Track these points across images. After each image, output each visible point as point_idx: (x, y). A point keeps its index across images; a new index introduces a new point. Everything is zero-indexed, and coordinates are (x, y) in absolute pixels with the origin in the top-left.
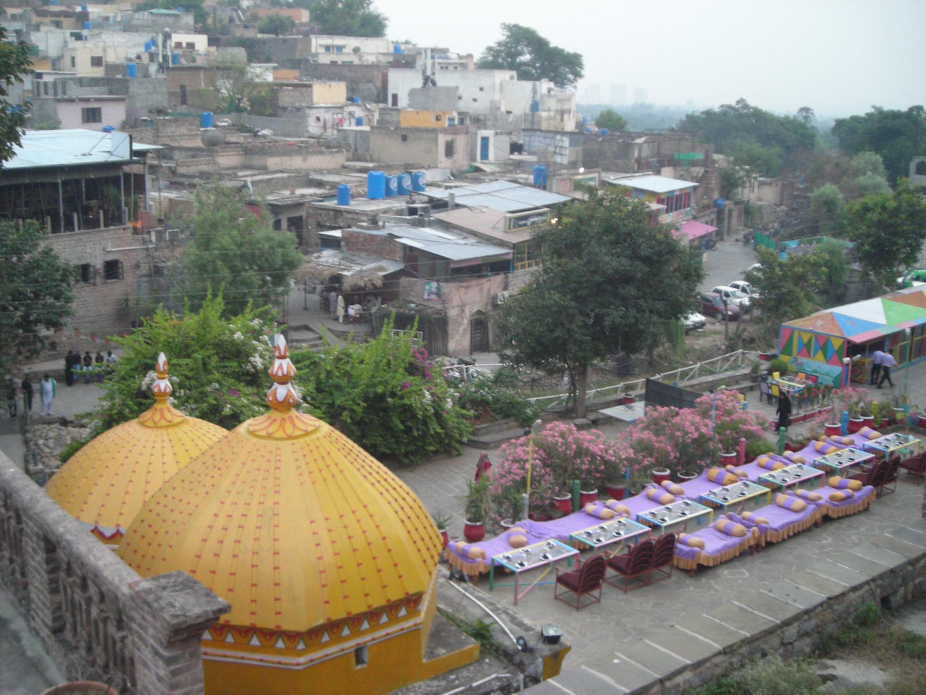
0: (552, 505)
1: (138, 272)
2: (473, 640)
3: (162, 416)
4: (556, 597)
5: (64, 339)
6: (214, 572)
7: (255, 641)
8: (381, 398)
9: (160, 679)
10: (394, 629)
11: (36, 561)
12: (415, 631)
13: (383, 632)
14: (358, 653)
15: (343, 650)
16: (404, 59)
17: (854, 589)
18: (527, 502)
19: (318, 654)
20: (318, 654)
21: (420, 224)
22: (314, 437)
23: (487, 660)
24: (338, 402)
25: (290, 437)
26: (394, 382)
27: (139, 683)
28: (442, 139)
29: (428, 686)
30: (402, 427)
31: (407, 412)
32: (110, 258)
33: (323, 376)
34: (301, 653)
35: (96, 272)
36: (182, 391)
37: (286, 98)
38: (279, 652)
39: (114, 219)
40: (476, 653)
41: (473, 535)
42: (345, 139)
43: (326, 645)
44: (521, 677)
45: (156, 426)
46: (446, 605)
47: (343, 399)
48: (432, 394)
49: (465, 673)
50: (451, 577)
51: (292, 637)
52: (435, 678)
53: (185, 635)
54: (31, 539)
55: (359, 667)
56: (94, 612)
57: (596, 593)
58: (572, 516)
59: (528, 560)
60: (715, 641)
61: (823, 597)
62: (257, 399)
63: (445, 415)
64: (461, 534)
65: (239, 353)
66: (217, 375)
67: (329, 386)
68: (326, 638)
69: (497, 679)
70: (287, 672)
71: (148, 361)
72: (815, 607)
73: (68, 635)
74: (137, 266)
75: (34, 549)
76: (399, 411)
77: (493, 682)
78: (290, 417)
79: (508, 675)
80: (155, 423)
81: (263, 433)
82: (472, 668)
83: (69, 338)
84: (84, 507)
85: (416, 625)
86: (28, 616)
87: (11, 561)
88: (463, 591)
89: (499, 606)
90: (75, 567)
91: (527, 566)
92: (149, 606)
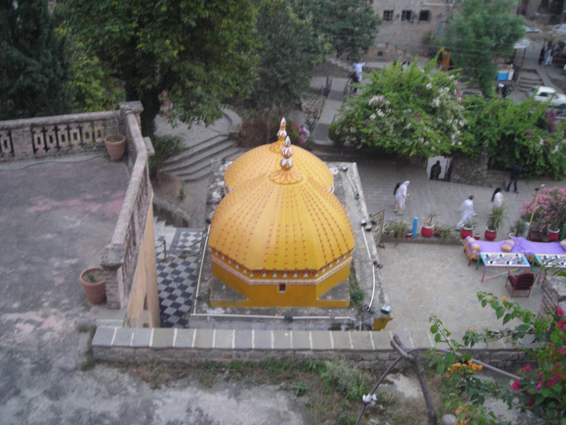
0: (545, 232)
2: (349, 298)
3: (278, 147)
4: (506, 286)
5: (388, 51)
8: (512, 136)
10: (300, 281)
12: (313, 286)
13: (295, 281)
18: (528, 228)
19: (260, 281)
20: (260, 281)
22: (292, 186)
23: (353, 309)
24: (485, 134)
25: (281, 183)
26: (521, 130)
30: (518, 156)
31: (525, 149)
32: (425, 9)
33: (482, 116)
34: (251, 278)
35: (415, 17)
36: (390, 110)
38: (244, 274)
40: (348, 304)
41: (490, 237)
43: (264, 278)
44: (361, 323)
45: (274, 151)
47: (488, 132)
48: (545, 142)
49: (338, 311)
50: (375, 263)
51: (248, 271)
55: (282, 292)
57: (528, 292)
58: (552, 244)
59: (498, 260)
60: (335, 344)
62: (430, 123)
63: (549, 156)
64: (482, 235)
65: (429, 95)
66: (412, 105)
67: (486, 122)
68: (264, 275)
69: (349, 320)
74: (440, 16)
76: (521, 147)
79: (355, 320)
81: (272, 178)
82: (343, 310)
83: (391, 51)
88: (374, 272)
89: (382, 286)
91: (494, 264)
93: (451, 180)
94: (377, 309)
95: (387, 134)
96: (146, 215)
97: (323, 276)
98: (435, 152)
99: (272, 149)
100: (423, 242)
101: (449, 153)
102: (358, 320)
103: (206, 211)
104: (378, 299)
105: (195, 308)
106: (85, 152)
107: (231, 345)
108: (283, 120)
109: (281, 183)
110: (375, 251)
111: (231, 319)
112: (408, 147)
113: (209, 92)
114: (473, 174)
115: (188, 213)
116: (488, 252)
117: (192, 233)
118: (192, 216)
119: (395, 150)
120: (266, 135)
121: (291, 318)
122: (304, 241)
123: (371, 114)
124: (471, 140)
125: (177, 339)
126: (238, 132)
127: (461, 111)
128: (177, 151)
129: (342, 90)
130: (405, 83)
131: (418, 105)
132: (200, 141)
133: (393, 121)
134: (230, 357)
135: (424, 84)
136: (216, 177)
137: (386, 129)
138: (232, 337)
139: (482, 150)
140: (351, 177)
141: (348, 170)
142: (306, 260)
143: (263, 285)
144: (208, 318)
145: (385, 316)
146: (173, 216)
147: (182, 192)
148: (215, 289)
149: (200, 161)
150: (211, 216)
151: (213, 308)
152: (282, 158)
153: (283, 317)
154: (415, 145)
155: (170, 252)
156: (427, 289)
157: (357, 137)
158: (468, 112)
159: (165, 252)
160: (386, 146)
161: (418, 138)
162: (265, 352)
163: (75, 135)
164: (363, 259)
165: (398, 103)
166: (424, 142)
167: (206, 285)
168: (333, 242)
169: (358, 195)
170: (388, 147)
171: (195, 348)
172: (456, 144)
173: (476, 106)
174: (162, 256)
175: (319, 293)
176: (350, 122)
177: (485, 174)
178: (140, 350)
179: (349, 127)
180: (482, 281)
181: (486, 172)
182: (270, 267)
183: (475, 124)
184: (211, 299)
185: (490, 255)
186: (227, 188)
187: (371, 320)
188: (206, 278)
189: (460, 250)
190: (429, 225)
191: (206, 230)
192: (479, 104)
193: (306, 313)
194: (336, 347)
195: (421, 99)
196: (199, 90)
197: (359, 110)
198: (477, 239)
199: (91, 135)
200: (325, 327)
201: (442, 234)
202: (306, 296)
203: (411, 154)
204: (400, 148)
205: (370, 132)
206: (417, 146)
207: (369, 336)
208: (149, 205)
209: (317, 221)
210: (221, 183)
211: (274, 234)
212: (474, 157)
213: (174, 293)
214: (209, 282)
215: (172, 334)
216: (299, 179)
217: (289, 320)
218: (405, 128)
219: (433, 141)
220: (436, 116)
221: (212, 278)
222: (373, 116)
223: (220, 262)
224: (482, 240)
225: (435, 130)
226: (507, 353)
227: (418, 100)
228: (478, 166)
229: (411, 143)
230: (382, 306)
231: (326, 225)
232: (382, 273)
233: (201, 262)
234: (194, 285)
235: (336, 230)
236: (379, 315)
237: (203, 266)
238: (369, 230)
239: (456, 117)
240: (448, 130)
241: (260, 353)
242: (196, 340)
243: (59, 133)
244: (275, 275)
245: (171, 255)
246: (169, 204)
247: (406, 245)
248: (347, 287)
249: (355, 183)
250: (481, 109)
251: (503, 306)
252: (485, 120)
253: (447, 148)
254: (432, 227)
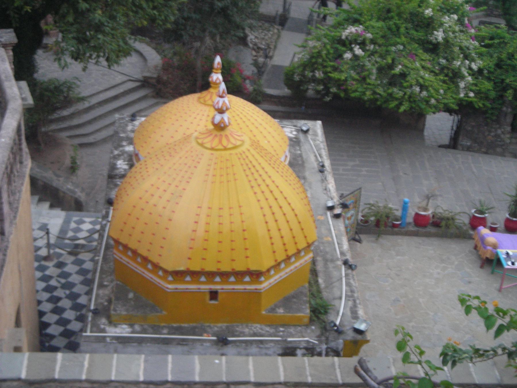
2: (308, 311)
6: (138, 219)
12: (257, 293)
15: (199, 289)
19: (181, 286)
20: (181, 286)
22: (228, 152)
23: (313, 327)
24: (507, 81)
25: (212, 149)
29: (261, 329)
33: (504, 56)
34: (170, 282)
36: (372, 47)
38: (160, 277)
40: (306, 320)
44: (324, 347)
45: (205, 104)
46: (325, 281)
47: (512, 79)
49: (292, 330)
50: (346, 263)
51: (165, 271)
52: (269, 326)
55: (213, 302)
60: (285, 376)
62: (429, 66)
64: (501, 225)
65: (429, 25)
66: (403, 39)
67: (509, 65)
69: (308, 342)
70: (162, 290)
71: (358, 17)
77: (303, 342)
78: (221, 135)
79: (316, 342)
80: (205, 101)
81: (200, 141)
82: (299, 328)
84: (144, 145)
85: (256, 289)
88: (344, 274)
89: (356, 295)
93: (460, 147)
94: (348, 328)
95: (368, 81)
96: (20, 192)
97: (272, 280)
98: (435, 107)
99: (202, 100)
100: (416, 234)
101: (456, 108)
102: (320, 342)
103: (108, 187)
104: (349, 313)
105: (89, 326)
107: (138, 376)
108: (218, 59)
109: (212, 149)
110: (346, 246)
111: (140, 341)
112: (397, 99)
113: (112, 18)
114: (490, 138)
115: (83, 190)
116: (509, 249)
117: (87, 220)
118: (88, 194)
119: (379, 103)
120: (196, 80)
121: (226, 339)
122: (244, 230)
123: (345, 52)
124: (488, 90)
125: (61, 368)
126: (155, 76)
127: (475, 48)
128: (68, 102)
129: (305, 17)
130: (394, 8)
131: (413, 39)
132: (101, 89)
133: (377, 62)
135: (420, 10)
136: (122, 139)
137: (366, 73)
138: (139, 365)
139: (503, 103)
140: (314, 140)
141: (310, 132)
142: (247, 257)
143: (185, 292)
144: (108, 340)
145: (359, 337)
146: (61, 194)
147: (74, 161)
148: (117, 299)
149: (101, 117)
150: (113, 194)
151: (115, 326)
152: (216, 113)
153: (215, 338)
154: (406, 97)
155: (56, 246)
156: (421, 300)
157: (325, 85)
158: (484, 49)
159: (49, 246)
160: (366, 98)
161: (411, 86)
164: (329, 256)
165: (383, 37)
166: (421, 92)
167: (106, 292)
168: (285, 232)
169: (323, 166)
170: (370, 100)
171: (87, 381)
172: (466, 95)
173: (496, 41)
174: (43, 252)
175: (266, 304)
176: (316, 63)
177: (507, 138)
178: (8, 383)
179: (313, 71)
180: (500, 290)
181: (508, 136)
182: (196, 268)
183: (493, 67)
184: (112, 312)
185: (511, 253)
186: (137, 155)
187: (340, 344)
188: (106, 283)
189: (468, 246)
190: (425, 210)
191: (107, 214)
192: (501, 38)
193: (246, 332)
194: (287, 380)
195: (417, 31)
196: (98, 15)
197: (328, 47)
198: (493, 230)
200: (275, 352)
201: (443, 223)
202: (247, 308)
203: (402, 109)
204: (386, 101)
205: (343, 78)
206: (410, 97)
207: (333, 365)
208: (24, 176)
209: (263, 203)
210: (129, 149)
211: (203, 219)
212: (492, 114)
213: (60, 304)
214: (109, 288)
215: (55, 361)
216: (239, 143)
217: (222, 341)
218: (393, 72)
219: (432, 91)
220: (437, 55)
221: (115, 282)
222: (348, 55)
223: (125, 260)
224: (500, 232)
225: (436, 74)
227: (413, 32)
228: (498, 126)
229: (401, 94)
230: (354, 323)
231: (276, 209)
232: (355, 277)
233: (98, 260)
234: (89, 293)
235: (290, 215)
236: (350, 335)
237: (102, 264)
238: (337, 216)
239: (466, 57)
240: (455, 76)
242: (88, 369)
244: (203, 279)
245: (58, 250)
246: (55, 178)
247: (391, 237)
248: (306, 296)
249: (319, 149)
250: (502, 45)
251: (495, 314)
252: (509, 62)
253: (453, 101)
254: (429, 213)
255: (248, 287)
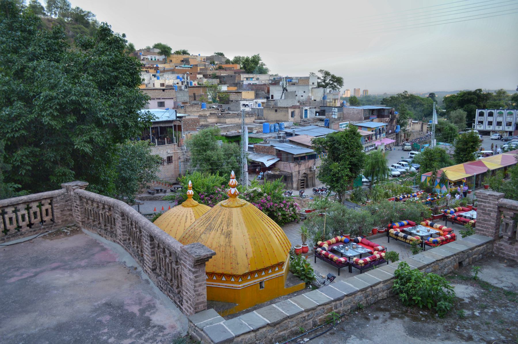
1: (180, 161)
7: (224, 279)
9: (191, 279)
11: (147, 244)
12: (282, 276)
14: (261, 283)
16: (276, 82)
17: (447, 258)
21: (283, 142)
27: (183, 282)
28: (290, 111)
32: (169, 155)
34: (240, 283)
37: (233, 97)
38: (232, 283)
39: (171, 141)
42: (254, 112)
45: (188, 206)
51: (237, 277)
53: (201, 262)
54: (145, 237)
56: (167, 260)
61: (435, 260)
70: (234, 290)
72: (431, 264)
73: (158, 271)
75: (146, 241)
86: (143, 266)
87: (137, 247)
90: (161, 245)
92: (188, 253)
106: (35, 231)
134: (331, 309)
162: (353, 296)
163: (23, 216)
178: (261, 331)
199: (38, 214)
226: (479, 248)
241: (350, 297)
243: (6, 216)
255: (278, 274)
